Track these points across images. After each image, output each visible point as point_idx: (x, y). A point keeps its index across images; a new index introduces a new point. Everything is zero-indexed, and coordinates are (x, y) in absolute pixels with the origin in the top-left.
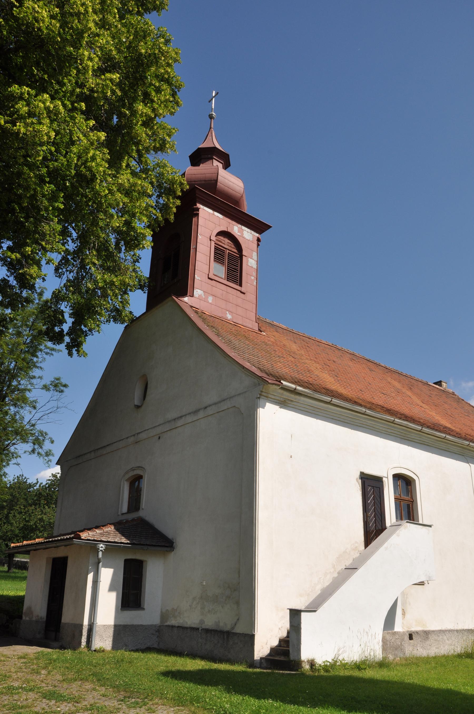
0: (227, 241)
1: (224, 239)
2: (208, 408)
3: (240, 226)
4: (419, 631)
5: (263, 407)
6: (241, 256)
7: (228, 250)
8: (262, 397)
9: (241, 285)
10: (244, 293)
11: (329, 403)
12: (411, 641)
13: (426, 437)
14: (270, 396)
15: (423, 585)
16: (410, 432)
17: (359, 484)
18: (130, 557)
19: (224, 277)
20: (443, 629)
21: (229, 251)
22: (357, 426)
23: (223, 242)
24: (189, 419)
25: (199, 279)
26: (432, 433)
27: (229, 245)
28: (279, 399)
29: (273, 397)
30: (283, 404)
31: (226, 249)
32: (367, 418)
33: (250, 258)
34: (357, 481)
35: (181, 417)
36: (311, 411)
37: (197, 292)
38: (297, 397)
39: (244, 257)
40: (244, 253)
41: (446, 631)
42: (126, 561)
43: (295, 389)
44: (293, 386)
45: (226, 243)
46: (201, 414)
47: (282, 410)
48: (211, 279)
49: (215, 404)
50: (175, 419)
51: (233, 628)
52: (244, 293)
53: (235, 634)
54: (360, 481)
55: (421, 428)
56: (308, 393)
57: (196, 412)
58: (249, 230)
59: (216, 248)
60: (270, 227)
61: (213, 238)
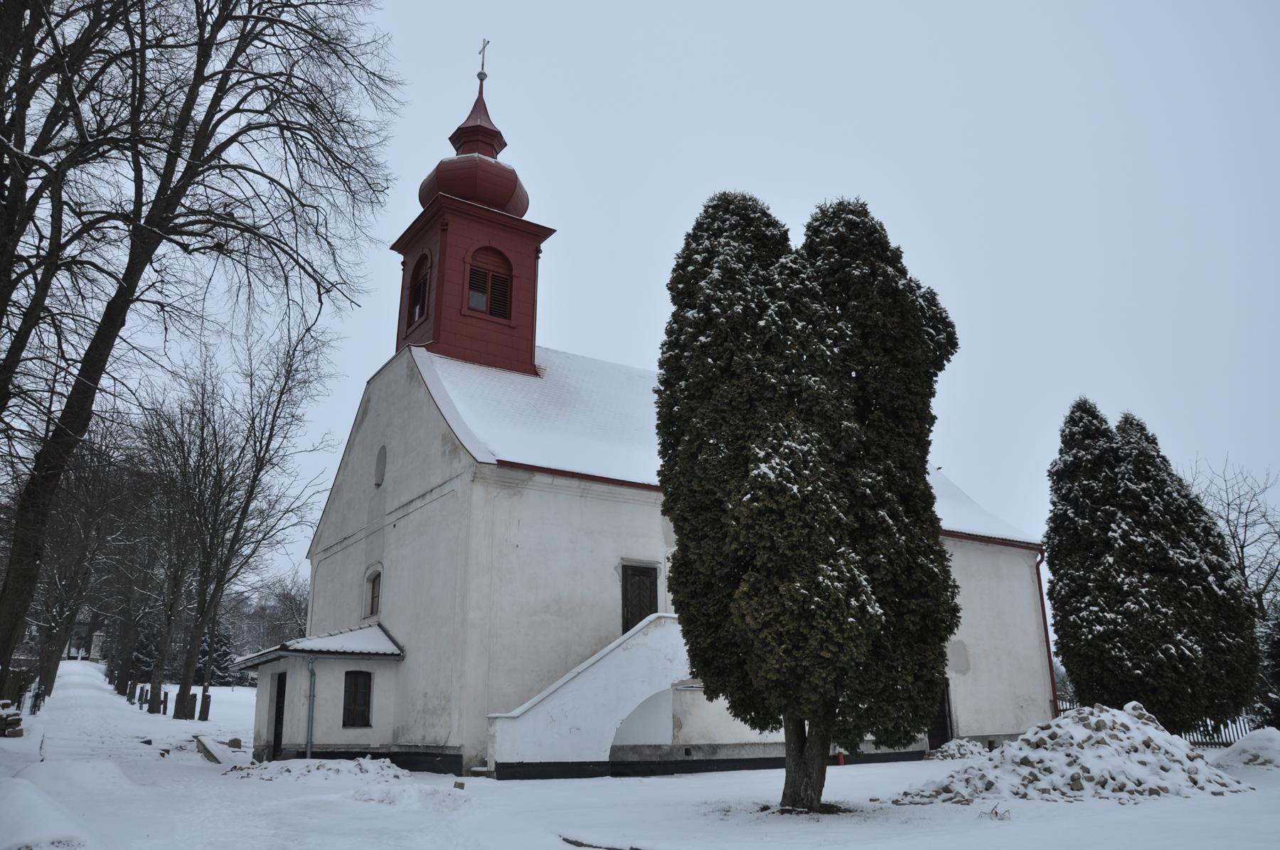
2: (434, 491)
6: (511, 277)
9: (510, 320)
10: (514, 328)
18: (354, 666)
19: (484, 309)
20: (743, 742)
24: (418, 504)
34: (616, 568)
35: (412, 501)
39: (515, 279)
40: (515, 273)
41: (746, 744)
42: (347, 673)
46: (428, 498)
48: (465, 316)
49: (440, 486)
50: (407, 504)
51: (446, 742)
52: (514, 328)
53: (447, 747)
57: (423, 495)
59: (472, 272)
60: (555, 231)
61: (469, 259)
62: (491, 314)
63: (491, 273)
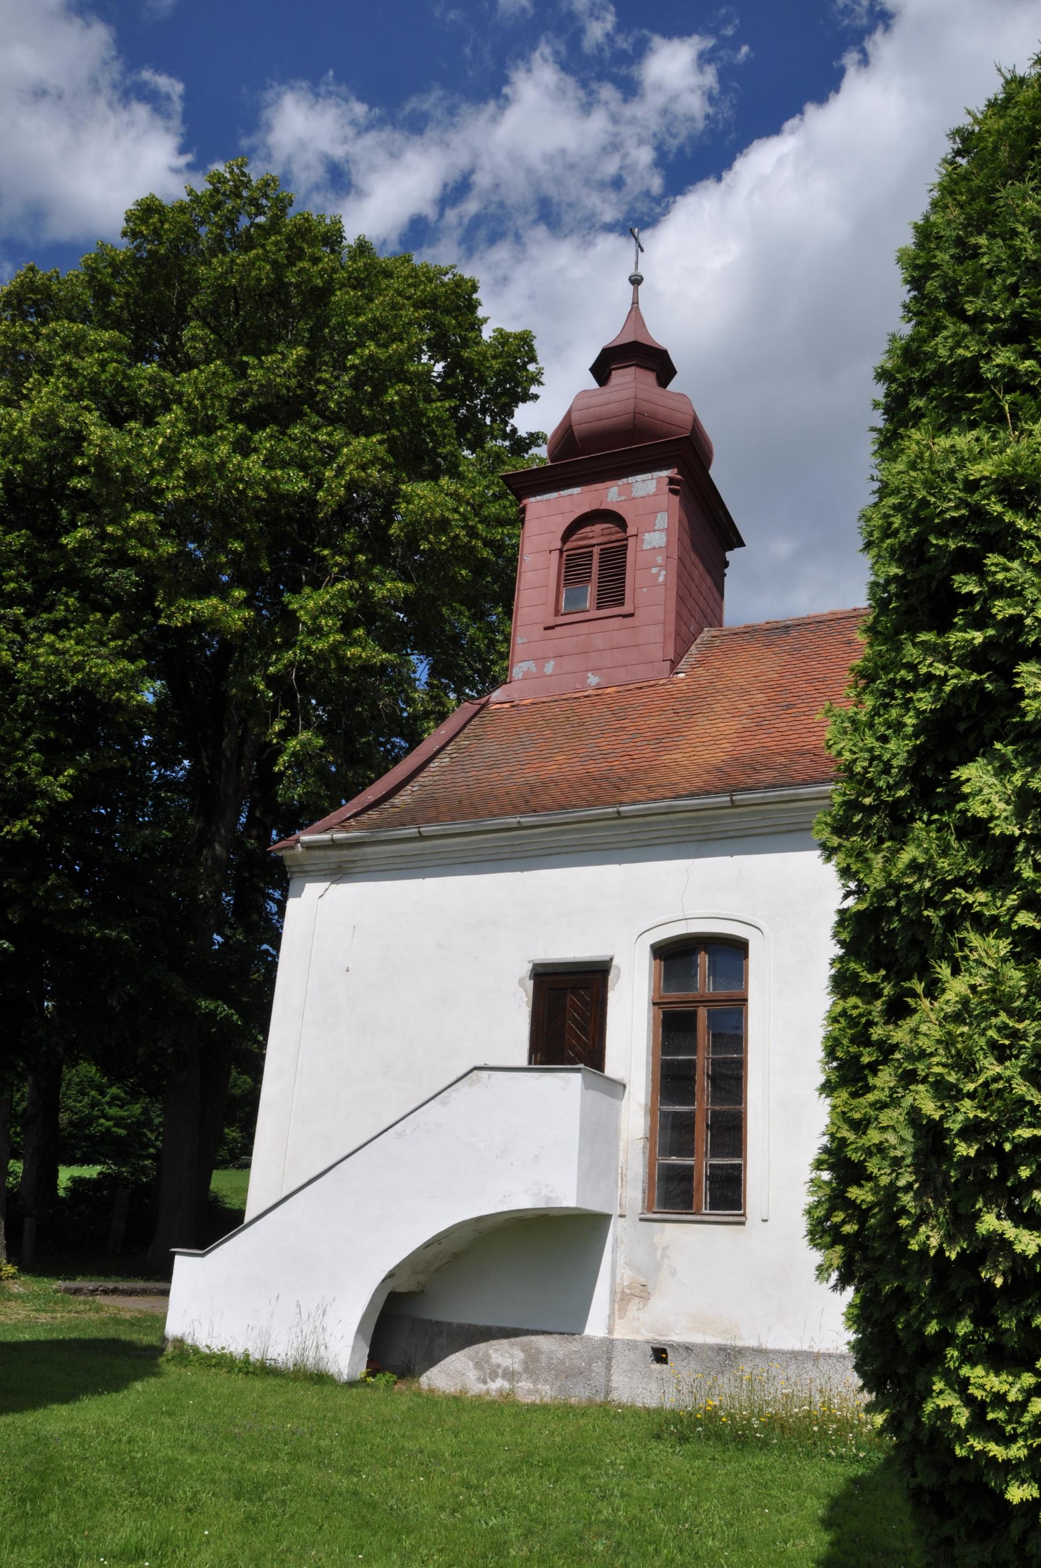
0: (598, 528)
1: (594, 528)
3: (625, 480)
4: (695, 1345)
5: (298, 895)
7: (598, 544)
8: (296, 875)
10: (632, 615)
11: (422, 838)
12: (657, 1366)
13: (782, 811)
14: (307, 868)
15: (743, 1223)
16: (713, 818)
17: (526, 991)
21: (602, 547)
22: (539, 856)
23: (590, 535)
25: (525, 640)
26: (782, 796)
27: (605, 532)
28: (327, 867)
29: (314, 868)
30: (339, 873)
31: (593, 546)
32: (552, 832)
33: (649, 532)
34: (521, 982)
36: (404, 866)
37: (519, 670)
38: (355, 851)
43: (332, 840)
44: (326, 837)
45: (597, 534)
47: (341, 886)
52: (632, 615)
54: (530, 984)
55: (728, 798)
56: (361, 837)
58: (648, 476)
62: (598, 608)
63: (596, 550)
